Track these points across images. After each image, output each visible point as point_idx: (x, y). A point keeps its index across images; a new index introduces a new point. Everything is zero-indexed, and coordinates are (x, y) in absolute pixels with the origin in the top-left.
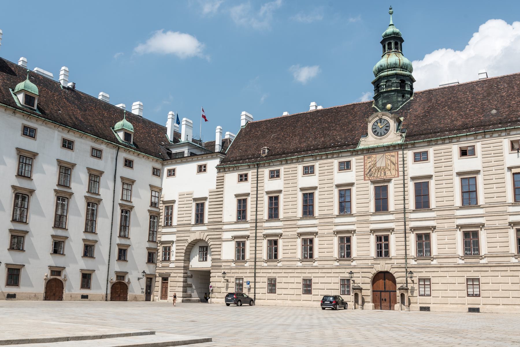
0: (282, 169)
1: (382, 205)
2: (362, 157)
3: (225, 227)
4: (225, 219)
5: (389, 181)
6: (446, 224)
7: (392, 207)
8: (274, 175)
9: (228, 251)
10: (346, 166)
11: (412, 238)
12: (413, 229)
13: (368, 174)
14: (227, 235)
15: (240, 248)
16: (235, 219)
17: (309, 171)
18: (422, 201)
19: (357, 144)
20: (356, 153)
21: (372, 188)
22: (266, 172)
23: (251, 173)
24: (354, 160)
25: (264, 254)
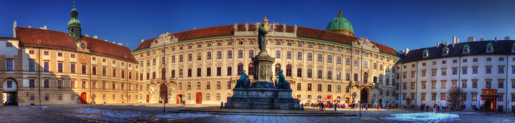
0: (50, 51)
1: (84, 72)
2: (78, 54)
3: (24, 73)
4: (24, 68)
5: (86, 64)
6: (99, 80)
7: (87, 73)
8: (46, 53)
9: (26, 83)
10: (73, 56)
11: (92, 82)
12: (93, 80)
13: (80, 60)
14: (24, 76)
15: (32, 82)
16: (28, 69)
17: (60, 55)
18: (94, 73)
19: (76, 49)
20: (77, 52)
21: (81, 65)
22: (43, 51)
23: (36, 51)
24: (76, 55)
25: (43, 84)
